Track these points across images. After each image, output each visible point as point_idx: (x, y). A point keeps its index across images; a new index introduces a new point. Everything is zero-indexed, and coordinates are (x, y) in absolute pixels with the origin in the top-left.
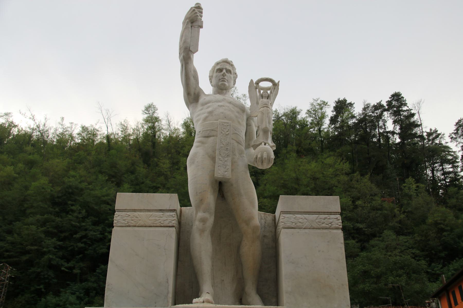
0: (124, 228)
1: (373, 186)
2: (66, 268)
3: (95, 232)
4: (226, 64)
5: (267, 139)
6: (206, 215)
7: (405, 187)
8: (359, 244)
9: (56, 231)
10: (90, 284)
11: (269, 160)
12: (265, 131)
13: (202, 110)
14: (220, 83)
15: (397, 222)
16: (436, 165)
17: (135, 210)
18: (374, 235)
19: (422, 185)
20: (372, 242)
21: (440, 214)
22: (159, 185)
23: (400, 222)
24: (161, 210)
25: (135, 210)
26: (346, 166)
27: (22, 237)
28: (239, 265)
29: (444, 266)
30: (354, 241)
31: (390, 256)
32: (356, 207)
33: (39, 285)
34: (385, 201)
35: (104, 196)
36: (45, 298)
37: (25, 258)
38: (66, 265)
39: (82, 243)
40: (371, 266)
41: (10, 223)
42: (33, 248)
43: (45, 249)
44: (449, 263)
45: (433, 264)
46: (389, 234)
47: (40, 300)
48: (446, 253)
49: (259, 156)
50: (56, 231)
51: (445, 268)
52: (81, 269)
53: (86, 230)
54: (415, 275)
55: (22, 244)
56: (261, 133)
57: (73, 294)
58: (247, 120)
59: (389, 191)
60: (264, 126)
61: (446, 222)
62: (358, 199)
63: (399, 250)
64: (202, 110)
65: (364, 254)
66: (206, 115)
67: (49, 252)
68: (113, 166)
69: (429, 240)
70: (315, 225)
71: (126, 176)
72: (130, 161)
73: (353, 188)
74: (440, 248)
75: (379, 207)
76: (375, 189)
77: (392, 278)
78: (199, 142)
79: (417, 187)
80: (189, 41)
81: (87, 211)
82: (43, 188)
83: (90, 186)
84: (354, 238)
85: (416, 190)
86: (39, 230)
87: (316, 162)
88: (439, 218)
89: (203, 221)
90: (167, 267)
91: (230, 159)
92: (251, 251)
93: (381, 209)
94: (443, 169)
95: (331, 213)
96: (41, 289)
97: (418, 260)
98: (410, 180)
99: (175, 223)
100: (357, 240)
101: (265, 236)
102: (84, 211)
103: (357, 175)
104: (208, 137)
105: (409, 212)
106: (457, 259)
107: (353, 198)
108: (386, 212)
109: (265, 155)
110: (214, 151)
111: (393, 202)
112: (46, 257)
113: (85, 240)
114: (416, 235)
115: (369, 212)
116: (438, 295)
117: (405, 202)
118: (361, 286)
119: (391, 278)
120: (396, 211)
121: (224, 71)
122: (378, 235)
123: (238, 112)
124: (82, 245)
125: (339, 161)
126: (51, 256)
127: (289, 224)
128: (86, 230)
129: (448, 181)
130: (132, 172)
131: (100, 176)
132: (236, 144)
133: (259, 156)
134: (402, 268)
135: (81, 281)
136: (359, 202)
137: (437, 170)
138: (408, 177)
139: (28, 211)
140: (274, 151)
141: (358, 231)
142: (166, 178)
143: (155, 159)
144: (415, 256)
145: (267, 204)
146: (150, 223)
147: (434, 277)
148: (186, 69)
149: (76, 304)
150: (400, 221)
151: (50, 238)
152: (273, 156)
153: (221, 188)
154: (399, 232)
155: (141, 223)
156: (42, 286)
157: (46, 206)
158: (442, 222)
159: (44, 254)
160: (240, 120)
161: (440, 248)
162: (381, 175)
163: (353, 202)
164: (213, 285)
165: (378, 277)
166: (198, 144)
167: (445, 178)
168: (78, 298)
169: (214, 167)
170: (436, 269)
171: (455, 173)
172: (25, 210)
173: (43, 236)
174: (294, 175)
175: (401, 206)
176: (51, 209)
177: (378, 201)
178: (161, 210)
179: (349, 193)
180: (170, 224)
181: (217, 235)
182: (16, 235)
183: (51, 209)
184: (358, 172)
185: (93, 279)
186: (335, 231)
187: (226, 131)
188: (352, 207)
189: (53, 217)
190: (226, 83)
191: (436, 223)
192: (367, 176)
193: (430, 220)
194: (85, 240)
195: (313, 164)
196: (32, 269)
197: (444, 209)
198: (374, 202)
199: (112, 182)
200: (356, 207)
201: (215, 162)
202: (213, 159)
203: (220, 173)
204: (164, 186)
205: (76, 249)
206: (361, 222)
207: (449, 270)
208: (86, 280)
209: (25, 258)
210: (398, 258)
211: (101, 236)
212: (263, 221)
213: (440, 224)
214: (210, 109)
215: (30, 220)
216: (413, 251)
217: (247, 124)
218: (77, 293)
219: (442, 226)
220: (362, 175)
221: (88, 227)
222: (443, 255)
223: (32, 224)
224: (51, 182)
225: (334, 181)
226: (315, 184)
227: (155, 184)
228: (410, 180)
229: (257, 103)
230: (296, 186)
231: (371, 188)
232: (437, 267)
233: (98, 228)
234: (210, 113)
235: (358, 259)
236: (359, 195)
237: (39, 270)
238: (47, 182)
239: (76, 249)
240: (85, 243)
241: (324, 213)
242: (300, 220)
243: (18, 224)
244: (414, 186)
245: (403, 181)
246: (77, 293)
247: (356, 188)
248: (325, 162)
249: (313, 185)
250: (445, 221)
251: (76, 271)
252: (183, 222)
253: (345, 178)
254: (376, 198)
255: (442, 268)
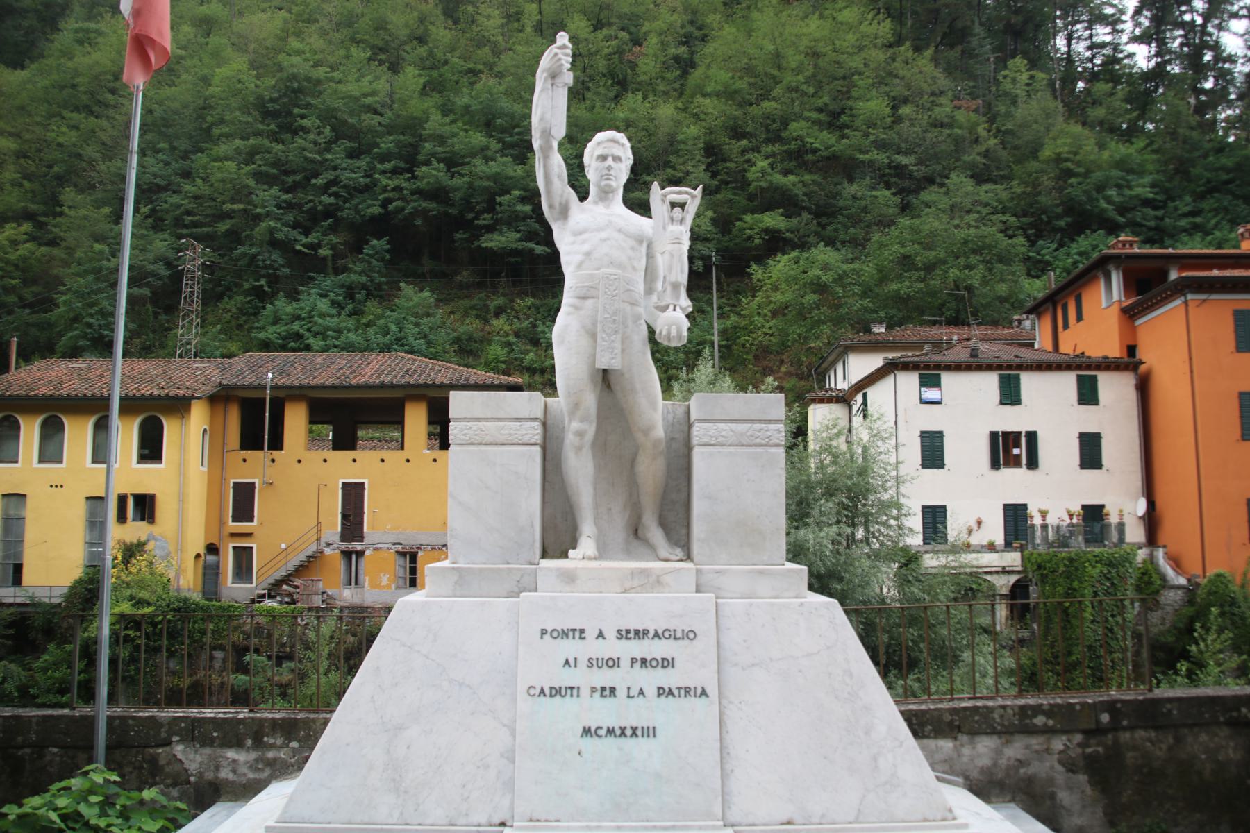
0: (465, 448)
1: (938, 74)
2: (303, 245)
3: (353, 171)
4: (612, 144)
5: (678, 298)
6: (584, 426)
7: (1005, 77)
8: (898, 199)
9: (275, 171)
10: (354, 277)
11: (680, 337)
12: (675, 286)
13: (573, 243)
14: (603, 183)
15: (979, 154)
16: (1079, 26)
17: (478, 420)
18: (930, 180)
19: (1040, 75)
20: (926, 196)
21: (1069, 140)
22: (480, 67)
23: (987, 154)
24: (517, 419)
25: (478, 420)
26: (885, 28)
27: (212, 185)
28: (633, 486)
29: (1061, 245)
30: (887, 193)
31: (957, 227)
32: (898, 120)
33: (258, 280)
34: (959, 108)
35: (365, 95)
36: (272, 304)
37: (223, 227)
38: (304, 240)
39: (330, 195)
40: (917, 246)
41: (185, 156)
42: (235, 207)
43: (259, 210)
44: (1073, 240)
45: (1041, 242)
46: (960, 182)
47: (264, 308)
48: (1069, 219)
49: (664, 333)
50: (275, 171)
51: (1063, 250)
52: (333, 248)
53: (335, 168)
54: (1000, 266)
55: (214, 200)
56: (669, 289)
57: (325, 296)
58: (648, 247)
59: (971, 84)
60: (673, 279)
61: (1078, 158)
62: (905, 101)
63: (976, 216)
64: (573, 243)
65: (904, 221)
66: (579, 258)
67: (268, 215)
68: (381, 26)
69: (1040, 193)
70: (746, 441)
71: (408, 48)
72: (416, 14)
73: (896, 76)
74: (1059, 210)
75: (946, 120)
76: (943, 82)
77: (956, 271)
78: (571, 306)
79: (1032, 77)
80: (548, 116)
81: (333, 129)
82: (239, 81)
83: (335, 74)
84: (888, 186)
85: (1028, 85)
86: (243, 171)
87: (821, 17)
88: (1066, 149)
89: (581, 434)
90: (530, 505)
91: (619, 337)
92: (651, 471)
93: (950, 126)
94: (1091, 36)
95: (770, 422)
96: (262, 286)
97: (1011, 237)
98: (1019, 62)
99: (538, 438)
100: (894, 190)
101: (672, 439)
102: (327, 130)
103: (905, 50)
104: (584, 298)
105: (1008, 132)
106: (1088, 232)
107: (894, 99)
108: (959, 131)
109: (674, 332)
110: (595, 324)
111: (976, 111)
112: (263, 225)
113: (334, 189)
114: (1015, 183)
115: (925, 132)
116: (1036, 309)
117: (1002, 109)
118: (894, 286)
119: (954, 273)
120: (981, 130)
121: (610, 161)
122: (938, 180)
123: (632, 248)
124: (332, 200)
125: (870, 16)
126: (272, 224)
127: (706, 440)
128: (335, 168)
129: (1099, 62)
130: (422, 40)
131: (354, 50)
132: (628, 308)
133: (664, 333)
134: (974, 252)
135: (337, 272)
136: (905, 110)
137: (1079, 38)
138: (1014, 57)
139: (216, 131)
140: (687, 316)
141: (900, 170)
142: (497, 53)
143: (470, 9)
144: (1006, 230)
145: (710, 110)
146: (502, 439)
147: (1037, 268)
148: (545, 166)
149: (331, 316)
150: (987, 151)
151: (265, 187)
152: (685, 333)
153: (605, 379)
154: (980, 177)
155: (488, 439)
156: (263, 282)
157: (250, 119)
158: (1071, 156)
159: (258, 218)
160: (635, 264)
161: (1059, 210)
162: (959, 48)
163: (894, 108)
164: (597, 518)
165: (929, 268)
166: (571, 309)
167: (1094, 56)
168: (334, 303)
169: (595, 348)
170: (1044, 252)
171: (1116, 47)
172: (209, 129)
173: (252, 183)
174: (771, 47)
175: (992, 121)
176: (261, 127)
177: (944, 109)
178: (517, 419)
179: (887, 89)
180: (533, 441)
181: (601, 446)
182: (199, 182)
183: (261, 127)
184: (908, 44)
185: (358, 267)
186: (774, 450)
187: (612, 288)
188: (889, 120)
189: (266, 142)
190: (613, 184)
191: (1058, 159)
192: (929, 53)
193: (1047, 153)
194: (334, 189)
195: (814, 23)
196: (241, 249)
197: (1077, 129)
198: (937, 110)
199: (381, 63)
200: (898, 120)
201: (595, 341)
202: (593, 336)
203: (602, 363)
204: (491, 69)
205: (320, 208)
206: (906, 153)
207: (1068, 254)
208: (345, 269)
209: (223, 227)
210: (972, 231)
211: (368, 180)
212: (670, 417)
213: (1067, 160)
214: (586, 247)
215: (223, 149)
216: (1004, 218)
217: (648, 255)
218: (332, 294)
219: (1069, 164)
220: (917, 49)
221: (339, 161)
222: (1062, 223)
223: (227, 159)
224: (253, 66)
225: (856, 62)
226: (816, 65)
227: (471, 66)
228: (1019, 62)
229: (664, 228)
230: (776, 72)
231: (934, 78)
232: (1047, 248)
233: (358, 163)
234: (588, 254)
235: (893, 231)
236: (907, 93)
237: (253, 251)
238: (245, 67)
239: (320, 208)
240: (336, 195)
241: (760, 421)
242: (724, 433)
243: (200, 159)
244: (1024, 77)
245: (1002, 63)
246: (332, 294)
247: (903, 78)
248: (840, 18)
249: (810, 71)
250: (1076, 154)
251: (325, 252)
252: (549, 422)
253: (879, 56)
254: (943, 100)
255: (1056, 250)
